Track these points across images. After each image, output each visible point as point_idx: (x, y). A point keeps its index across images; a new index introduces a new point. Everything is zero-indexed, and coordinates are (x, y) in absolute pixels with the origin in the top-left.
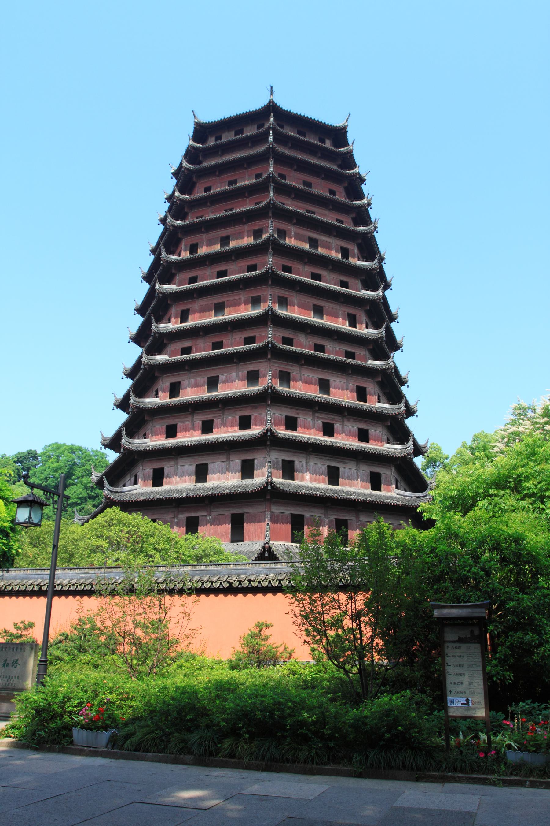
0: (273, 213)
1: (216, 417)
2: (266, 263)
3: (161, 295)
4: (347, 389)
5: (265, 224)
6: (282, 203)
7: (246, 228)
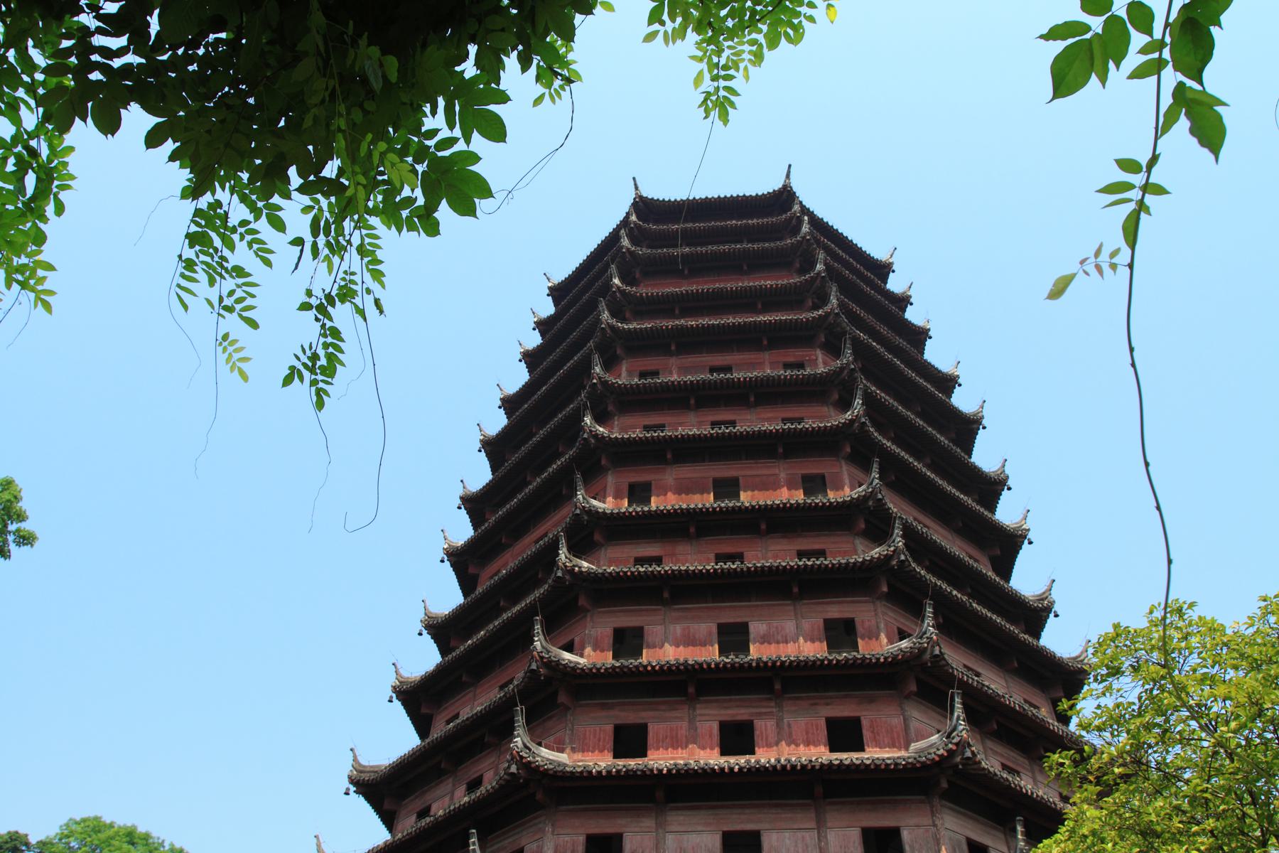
1: (760, 714)
7: (766, 356)
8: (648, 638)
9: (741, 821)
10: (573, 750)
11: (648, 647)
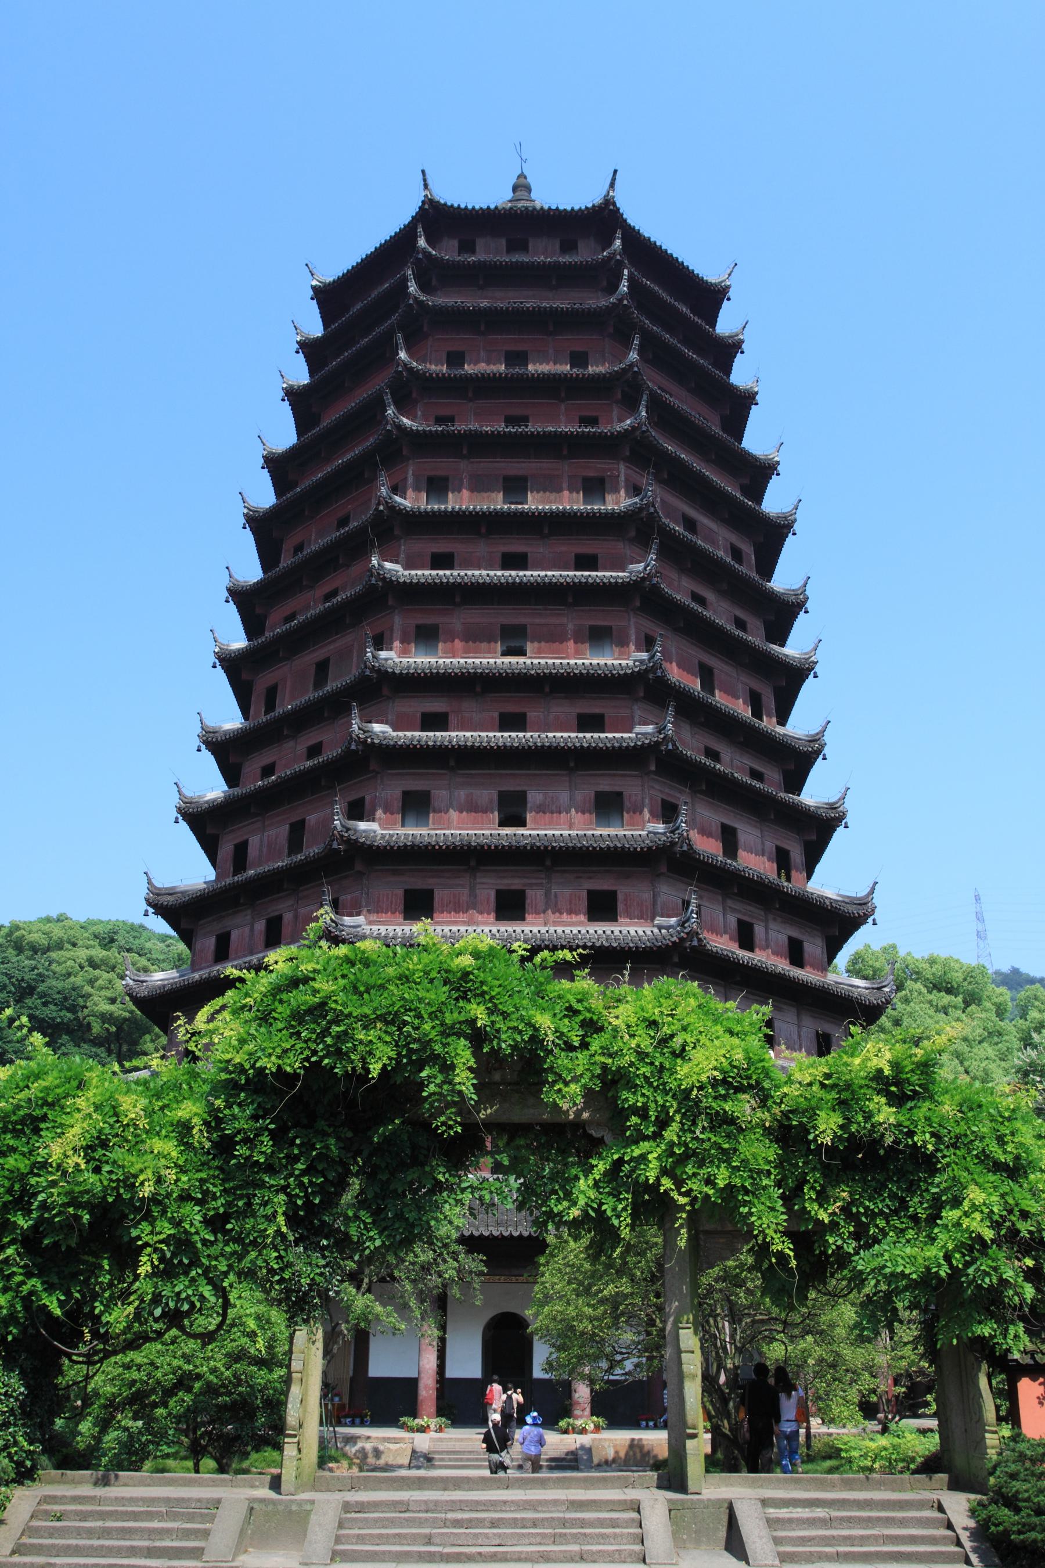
1: (531, 885)
3: (380, 584)
4: (763, 855)
5: (610, 470)
8: (435, 803)
10: (369, 911)
11: (434, 811)
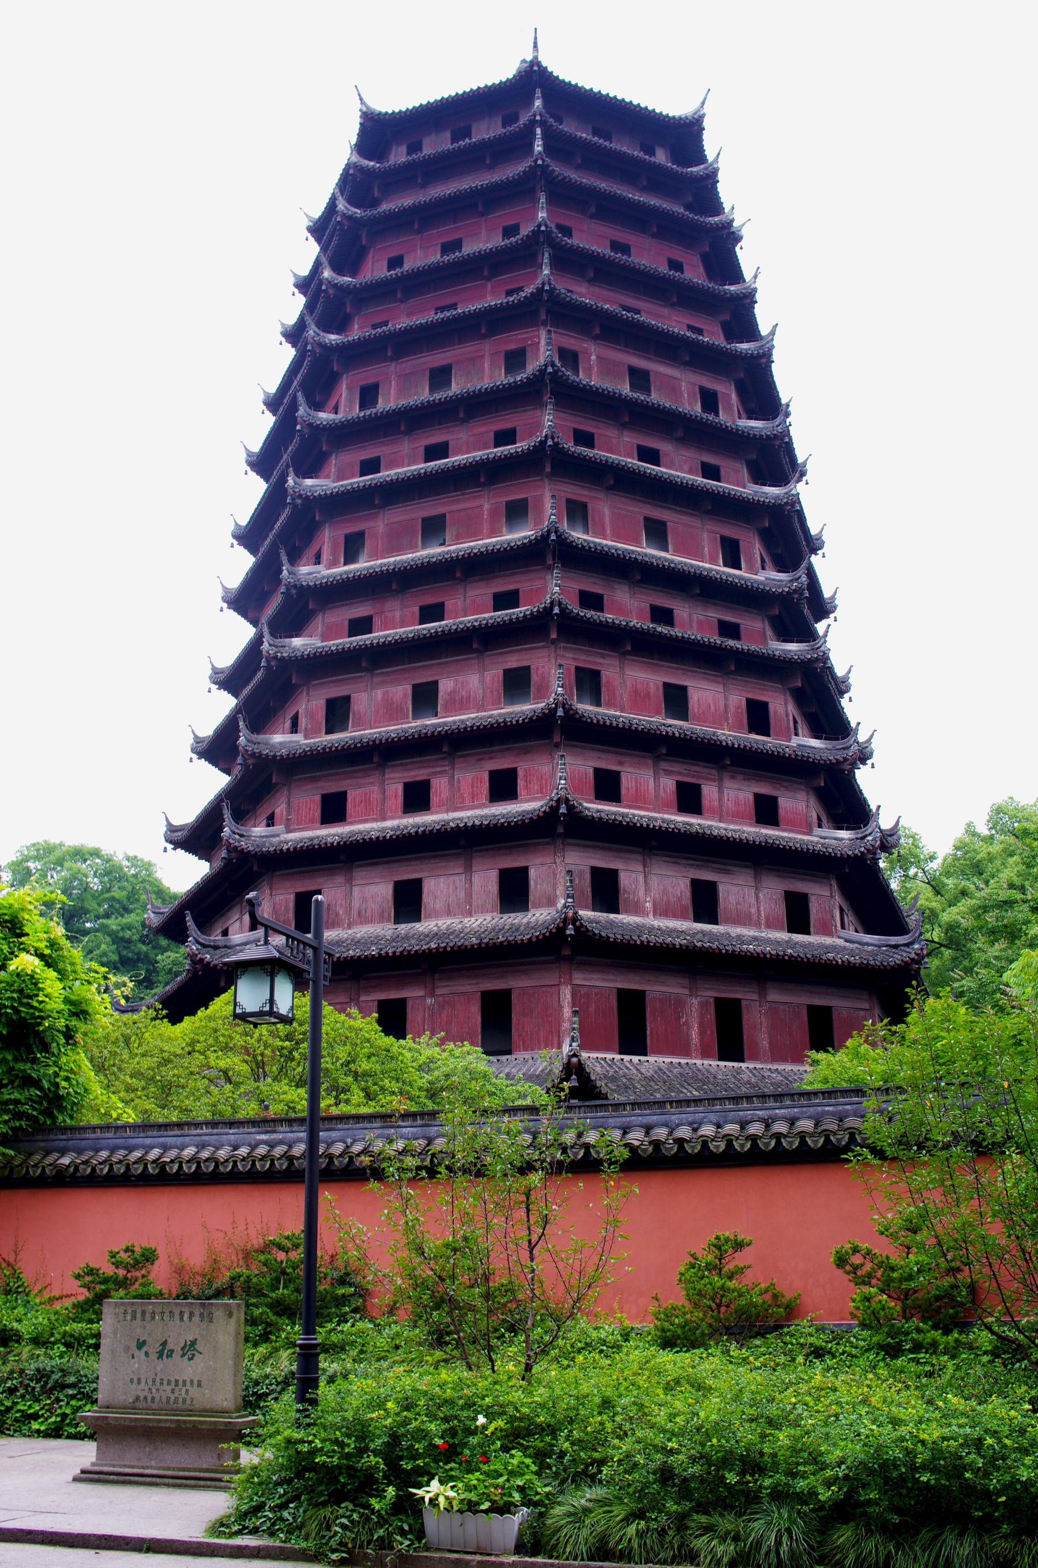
0: (548, 312)
1: (435, 773)
2: (539, 426)
3: (299, 501)
6: (569, 291)
7: (487, 347)
9: (407, 873)
